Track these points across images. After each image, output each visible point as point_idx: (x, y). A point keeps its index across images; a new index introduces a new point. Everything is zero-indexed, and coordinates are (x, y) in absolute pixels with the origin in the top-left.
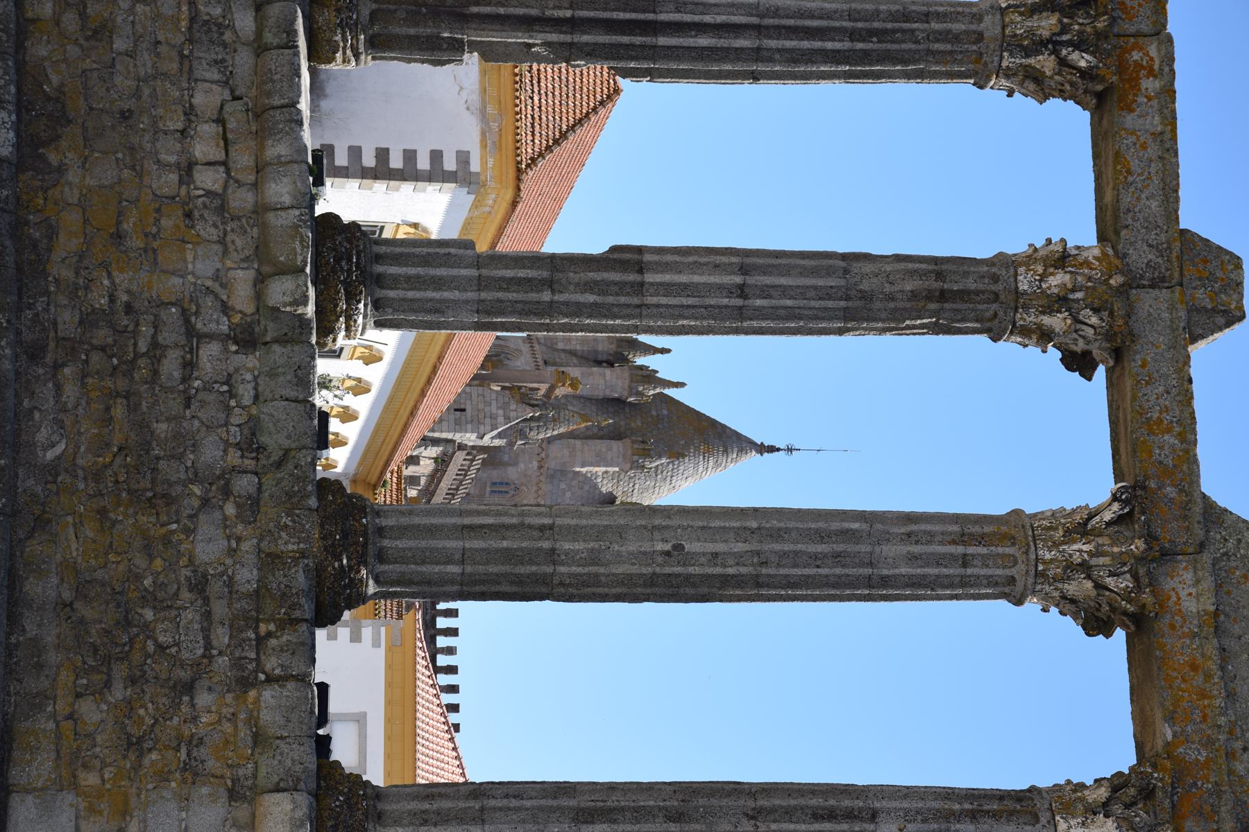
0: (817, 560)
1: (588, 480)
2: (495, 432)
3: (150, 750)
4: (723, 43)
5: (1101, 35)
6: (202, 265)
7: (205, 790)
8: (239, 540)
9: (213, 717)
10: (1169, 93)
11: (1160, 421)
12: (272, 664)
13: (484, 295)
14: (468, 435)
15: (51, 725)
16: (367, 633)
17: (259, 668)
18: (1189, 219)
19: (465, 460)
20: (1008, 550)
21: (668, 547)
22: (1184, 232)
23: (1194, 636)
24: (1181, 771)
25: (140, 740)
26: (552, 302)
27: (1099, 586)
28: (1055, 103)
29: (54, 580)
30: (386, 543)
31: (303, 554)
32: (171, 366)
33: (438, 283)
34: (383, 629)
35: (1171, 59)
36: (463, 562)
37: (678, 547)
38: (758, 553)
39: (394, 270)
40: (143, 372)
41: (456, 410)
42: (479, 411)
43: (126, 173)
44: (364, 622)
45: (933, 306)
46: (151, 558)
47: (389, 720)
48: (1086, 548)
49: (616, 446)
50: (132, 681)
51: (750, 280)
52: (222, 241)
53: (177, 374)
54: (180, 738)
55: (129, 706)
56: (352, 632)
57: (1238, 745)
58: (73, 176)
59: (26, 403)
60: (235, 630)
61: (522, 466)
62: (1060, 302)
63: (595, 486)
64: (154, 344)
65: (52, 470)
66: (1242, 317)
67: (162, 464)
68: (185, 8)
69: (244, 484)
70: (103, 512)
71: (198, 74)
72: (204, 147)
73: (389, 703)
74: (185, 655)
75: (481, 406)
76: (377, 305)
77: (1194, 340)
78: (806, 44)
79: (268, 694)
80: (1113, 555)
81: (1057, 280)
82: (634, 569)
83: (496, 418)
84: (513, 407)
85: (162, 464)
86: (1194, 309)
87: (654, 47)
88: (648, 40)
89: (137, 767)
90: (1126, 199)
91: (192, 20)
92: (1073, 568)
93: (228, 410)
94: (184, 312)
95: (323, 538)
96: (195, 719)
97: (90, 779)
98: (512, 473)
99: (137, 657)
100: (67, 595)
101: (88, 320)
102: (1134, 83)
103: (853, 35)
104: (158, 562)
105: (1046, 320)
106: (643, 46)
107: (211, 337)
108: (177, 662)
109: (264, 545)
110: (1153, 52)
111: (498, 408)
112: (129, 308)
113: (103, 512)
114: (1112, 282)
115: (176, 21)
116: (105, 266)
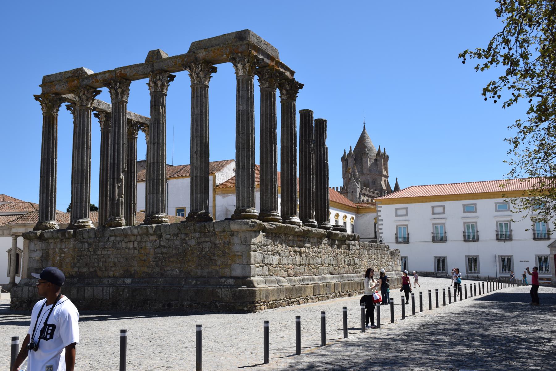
0: (197, 125)
1: (371, 165)
2: (357, 185)
4: (116, 150)
5: (114, 81)
10: (123, 68)
11: (175, 63)
12: (212, 229)
13: (155, 193)
16: (379, 209)
17: (212, 232)
18: (144, 62)
21: (195, 154)
22: (147, 61)
23: (209, 53)
24: (231, 53)
25: (223, 253)
26: (157, 180)
27: (201, 70)
28: (130, 88)
29: (198, 270)
31: (194, 225)
32: (164, 250)
33: (153, 202)
36: (198, 194)
37: (195, 152)
38: (196, 137)
39: (151, 210)
40: (165, 255)
43: (135, 259)
45: (157, 107)
46: (195, 253)
47: (397, 204)
48: (194, 74)
50: (214, 255)
51: (152, 142)
52: (145, 242)
53: (166, 249)
54: (223, 246)
55: (218, 255)
57: (227, 43)
58: (136, 268)
60: (206, 237)
61: (369, 179)
62: (155, 83)
63: (373, 163)
64: (161, 254)
65: (180, 271)
66: (158, 50)
67: (180, 251)
69: (183, 236)
70: (187, 262)
71: (120, 247)
72: (131, 245)
73: (393, 204)
74: (210, 246)
76: (157, 212)
77: (162, 58)
78: (117, 135)
79: (216, 230)
81: (152, 85)
82: (199, 161)
85: (180, 251)
86: (157, 58)
87: (118, 163)
89: (228, 253)
90: (140, 73)
92: (198, 77)
93: (171, 240)
94: (156, 248)
95: (191, 221)
96: (220, 243)
97: (230, 262)
98: (370, 181)
99: (210, 255)
100: (200, 268)
101: (157, 265)
102: (122, 74)
103: (115, 127)
104: (195, 251)
105: (159, 85)
106: (117, 165)
107: (160, 243)
108: (211, 247)
110: (118, 71)
112: (156, 258)
113: (187, 262)
115: (113, 251)
116: (149, 262)
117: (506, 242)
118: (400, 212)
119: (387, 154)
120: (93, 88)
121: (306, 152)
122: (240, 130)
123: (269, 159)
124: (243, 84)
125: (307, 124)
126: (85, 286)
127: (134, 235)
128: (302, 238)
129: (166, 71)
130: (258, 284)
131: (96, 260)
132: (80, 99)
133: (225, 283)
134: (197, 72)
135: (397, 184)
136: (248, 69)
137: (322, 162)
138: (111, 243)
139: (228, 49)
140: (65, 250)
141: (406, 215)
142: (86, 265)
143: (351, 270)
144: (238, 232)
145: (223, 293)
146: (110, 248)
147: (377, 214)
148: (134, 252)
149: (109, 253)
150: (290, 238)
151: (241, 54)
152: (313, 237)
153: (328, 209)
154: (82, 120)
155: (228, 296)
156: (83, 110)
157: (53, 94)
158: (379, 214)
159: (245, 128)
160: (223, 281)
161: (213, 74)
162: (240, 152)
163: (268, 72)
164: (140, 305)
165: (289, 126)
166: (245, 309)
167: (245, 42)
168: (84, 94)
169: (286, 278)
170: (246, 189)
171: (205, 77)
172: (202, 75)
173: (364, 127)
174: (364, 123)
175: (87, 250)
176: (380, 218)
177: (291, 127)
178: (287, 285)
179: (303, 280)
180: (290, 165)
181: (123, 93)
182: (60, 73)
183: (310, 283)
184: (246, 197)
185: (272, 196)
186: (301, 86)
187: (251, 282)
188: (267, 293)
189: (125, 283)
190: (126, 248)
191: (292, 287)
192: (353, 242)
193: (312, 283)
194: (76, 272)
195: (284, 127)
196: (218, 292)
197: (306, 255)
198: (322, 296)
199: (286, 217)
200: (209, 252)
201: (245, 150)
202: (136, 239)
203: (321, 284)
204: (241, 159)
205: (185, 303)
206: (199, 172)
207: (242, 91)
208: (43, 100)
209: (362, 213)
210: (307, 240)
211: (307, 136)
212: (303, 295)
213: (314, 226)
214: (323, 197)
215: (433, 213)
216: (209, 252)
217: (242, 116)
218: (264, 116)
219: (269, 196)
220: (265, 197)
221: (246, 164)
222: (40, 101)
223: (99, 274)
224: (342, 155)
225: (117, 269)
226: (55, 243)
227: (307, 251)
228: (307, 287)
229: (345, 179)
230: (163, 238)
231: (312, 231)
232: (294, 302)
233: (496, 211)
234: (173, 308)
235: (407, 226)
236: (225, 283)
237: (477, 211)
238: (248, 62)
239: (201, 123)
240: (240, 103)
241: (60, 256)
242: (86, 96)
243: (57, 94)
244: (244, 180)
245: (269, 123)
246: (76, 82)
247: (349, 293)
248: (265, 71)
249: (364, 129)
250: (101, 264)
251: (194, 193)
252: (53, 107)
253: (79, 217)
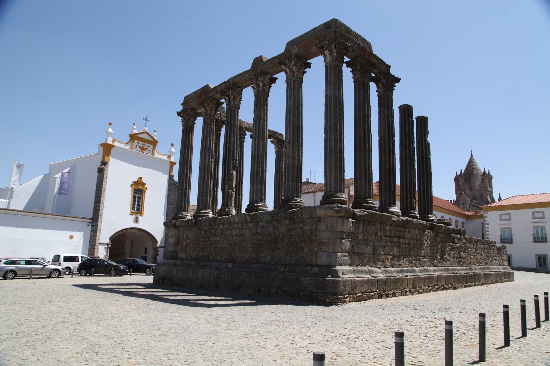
3: (312, 238)
4: (228, 148)
6: (248, 232)
7: (318, 227)
8: (283, 224)
9: (308, 227)
10: (235, 77)
12: (300, 216)
15: (307, 257)
20: (289, 83)
23: (301, 48)
25: (310, 240)
27: (294, 65)
30: (286, 196)
31: (285, 212)
32: (260, 237)
35: (231, 78)
45: (259, 105)
49: (472, 179)
53: (261, 236)
59: (263, 262)
64: (257, 240)
68: (220, 236)
69: (275, 223)
73: (497, 210)
79: (304, 216)
80: (289, 65)
82: (291, 149)
87: (228, 159)
88: (227, 160)
89: (315, 240)
90: (247, 79)
91: (221, 235)
93: (266, 227)
96: (308, 230)
100: (289, 255)
104: (285, 238)
109: (284, 219)
110: (231, 81)
112: (252, 245)
114: (255, 77)
118: (504, 217)
120: (216, 100)
121: (406, 145)
122: (328, 114)
123: (362, 146)
124: (330, 70)
125: (407, 118)
126: (198, 268)
127: (236, 223)
128: (402, 229)
129: (267, 74)
130: (343, 274)
131: (209, 245)
132: (205, 109)
133: (311, 272)
134: (291, 68)
136: (335, 54)
137: (424, 156)
138: (220, 231)
139: (317, 40)
140: (190, 236)
141: (510, 219)
142: (203, 249)
144: (324, 217)
145: (306, 281)
146: (219, 235)
147: (484, 219)
148: (236, 238)
149: (218, 239)
150: (386, 228)
151: (328, 42)
152: (414, 228)
154: (206, 127)
155: (312, 285)
156: (207, 118)
157: (190, 109)
158: (486, 219)
159: (333, 112)
160: (309, 270)
161: (307, 70)
162: (328, 137)
163: (360, 62)
164: (236, 289)
165: (386, 117)
166: (328, 300)
167: (332, 29)
168: (208, 105)
169: (381, 269)
170: (333, 174)
171: (298, 71)
172: (295, 69)
175: (203, 236)
176: (486, 222)
177: (388, 118)
178: (382, 276)
179: (402, 271)
180: (387, 155)
181: (235, 98)
182: (194, 92)
183: (409, 274)
184: (333, 182)
185: (366, 183)
186: (398, 80)
187: (336, 272)
188: (354, 284)
189: (228, 267)
190: (230, 235)
191: (387, 279)
193: (411, 274)
194: (196, 255)
195: (381, 119)
196: (302, 281)
198: (423, 288)
199: (384, 207)
200: (297, 239)
201: (333, 133)
202: (239, 226)
203: (421, 276)
204: (328, 142)
205: (272, 290)
206: (291, 161)
207: (330, 76)
208: (183, 115)
210: (407, 230)
211: (407, 130)
212: (401, 287)
213: (416, 217)
214: (426, 190)
215: (534, 218)
216: (297, 239)
217: (329, 101)
218: (357, 104)
219: (363, 183)
220: (358, 185)
221: (333, 148)
222: (181, 116)
223: (211, 258)
225: (224, 254)
226: (183, 231)
228: (405, 279)
230: (260, 226)
231: (412, 221)
232: (389, 294)
234: (262, 293)
235: (510, 228)
236: (311, 272)
238: (335, 48)
239: (293, 114)
240: (328, 88)
241: (186, 242)
242: (210, 107)
243: (192, 109)
244: (332, 165)
245: (362, 110)
246: (203, 96)
247: (454, 286)
248: (357, 61)
250: (212, 249)
251: (287, 181)
252: (190, 119)
253: (200, 208)
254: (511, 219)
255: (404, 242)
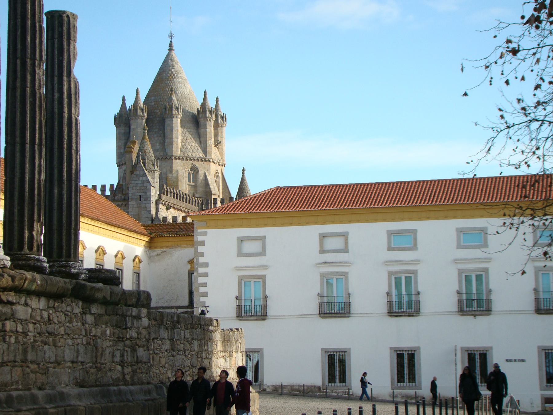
14: (152, 194)
16: (200, 238)
19: (167, 195)
34: (199, 231)
41: (140, 200)
42: (140, 189)
44: (195, 239)
56: (200, 245)
75: (138, 188)
83: (144, 181)
84: (138, 172)
111: (139, 180)
117: (479, 318)
118: (249, 247)
119: (223, 110)
135: (243, 181)
141: (263, 253)
143: (128, 377)
147: (196, 250)
153: (77, 229)
158: (200, 249)
173: (171, 45)
174: (171, 36)
176: (202, 260)
192: (135, 311)
197: (16, 338)
203: (51, 410)
209: (161, 247)
215: (322, 251)
224: (117, 110)
227: (20, 329)
229: (124, 168)
233: (459, 246)
235: (263, 278)
237: (419, 246)
249: (171, 50)
254: (267, 251)
255: (14, 329)
